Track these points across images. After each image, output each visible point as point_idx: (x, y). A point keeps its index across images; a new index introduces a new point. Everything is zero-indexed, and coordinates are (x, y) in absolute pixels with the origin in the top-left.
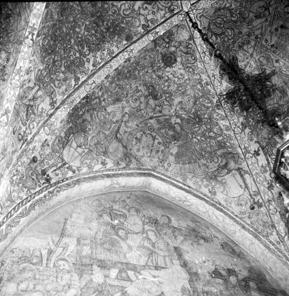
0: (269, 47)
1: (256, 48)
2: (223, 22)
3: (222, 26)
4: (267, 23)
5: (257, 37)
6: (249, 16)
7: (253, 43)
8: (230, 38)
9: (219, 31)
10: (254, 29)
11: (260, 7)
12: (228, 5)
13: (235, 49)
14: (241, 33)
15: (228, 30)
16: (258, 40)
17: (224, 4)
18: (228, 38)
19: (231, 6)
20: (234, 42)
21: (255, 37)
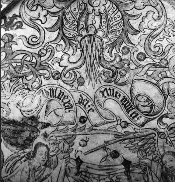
0: (72, 155)
1: (61, 128)
2: (91, 32)
3: (84, 33)
4: (119, 129)
5: (83, 120)
6: (121, 84)
7: (69, 116)
8: (64, 63)
9: (70, 33)
10: (101, 110)
11: (148, 100)
12: (135, 24)
13: (45, 82)
14: (82, 84)
15: (79, 52)
16: (80, 125)
17: (137, 12)
18: (61, 60)
19: (136, 32)
20: (58, 76)
21: (82, 117)
